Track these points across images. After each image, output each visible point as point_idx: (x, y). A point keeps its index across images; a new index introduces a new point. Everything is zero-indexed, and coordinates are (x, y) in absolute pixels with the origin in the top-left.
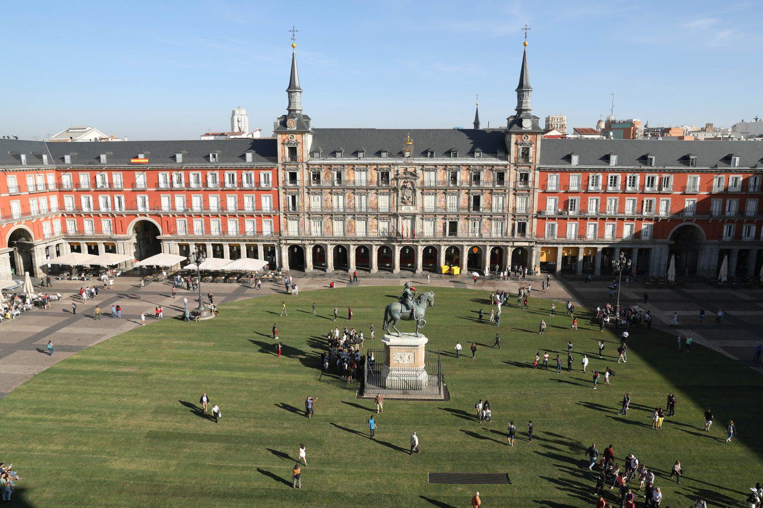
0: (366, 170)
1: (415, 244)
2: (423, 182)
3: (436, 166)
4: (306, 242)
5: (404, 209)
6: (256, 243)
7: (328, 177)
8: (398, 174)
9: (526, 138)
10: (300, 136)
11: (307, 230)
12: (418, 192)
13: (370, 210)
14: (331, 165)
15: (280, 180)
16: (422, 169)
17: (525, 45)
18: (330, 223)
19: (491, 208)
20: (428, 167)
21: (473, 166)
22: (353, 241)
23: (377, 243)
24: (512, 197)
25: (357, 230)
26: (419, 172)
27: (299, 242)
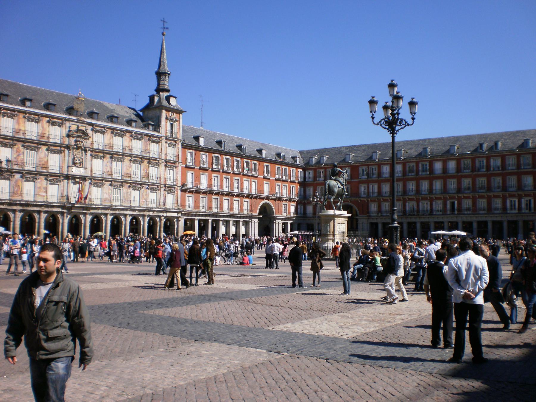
0: (37, 121)
2: (92, 144)
3: (104, 127)
5: (75, 171)
8: (70, 131)
12: (89, 153)
13: (40, 170)
16: (92, 130)
17: (163, 34)
21: (136, 133)
23: (46, 209)
24: (163, 167)
25: (25, 192)
26: (89, 132)
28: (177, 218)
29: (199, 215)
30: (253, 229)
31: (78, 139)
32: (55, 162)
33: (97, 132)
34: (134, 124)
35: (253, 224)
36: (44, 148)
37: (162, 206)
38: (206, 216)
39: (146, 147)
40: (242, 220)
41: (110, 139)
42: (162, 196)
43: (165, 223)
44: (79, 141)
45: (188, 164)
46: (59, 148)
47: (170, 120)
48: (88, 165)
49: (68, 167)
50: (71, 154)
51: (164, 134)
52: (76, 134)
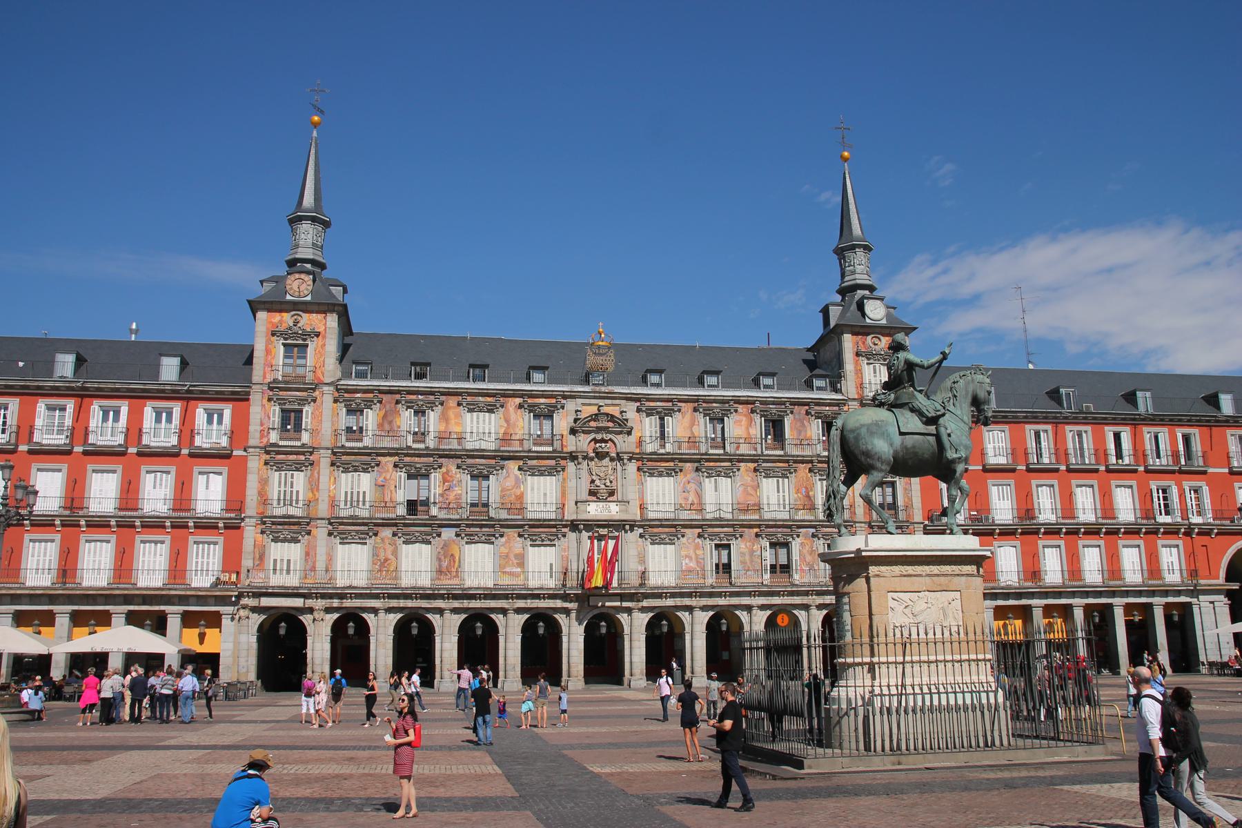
1: (625, 604)
2: (640, 442)
4: (319, 604)
5: (595, 510)
6: (162, 608)
7: (390, 423)
8: (576, 420)
9: (877, 341)
10: (320, 316)
11: (321, 565)
13: (504, 515)
14: (399, 392)
15: (254, 428)
18: (390, 549)
19: (812, 508)
20: (652, 404)
21: (762, 403)
22: (456, 597)
23: (521, 604)
27: (298, 602)
31: (599, 437)
32: (541, 495)
36: (513, 466)
38: (1019, 596)
39: (800, 432)
41: (692, 424)
44: (603, 441)
46: (553, 462)
48: (632, 494)
49: (576, 503)
50: (584, 473)
52: (593, 424)
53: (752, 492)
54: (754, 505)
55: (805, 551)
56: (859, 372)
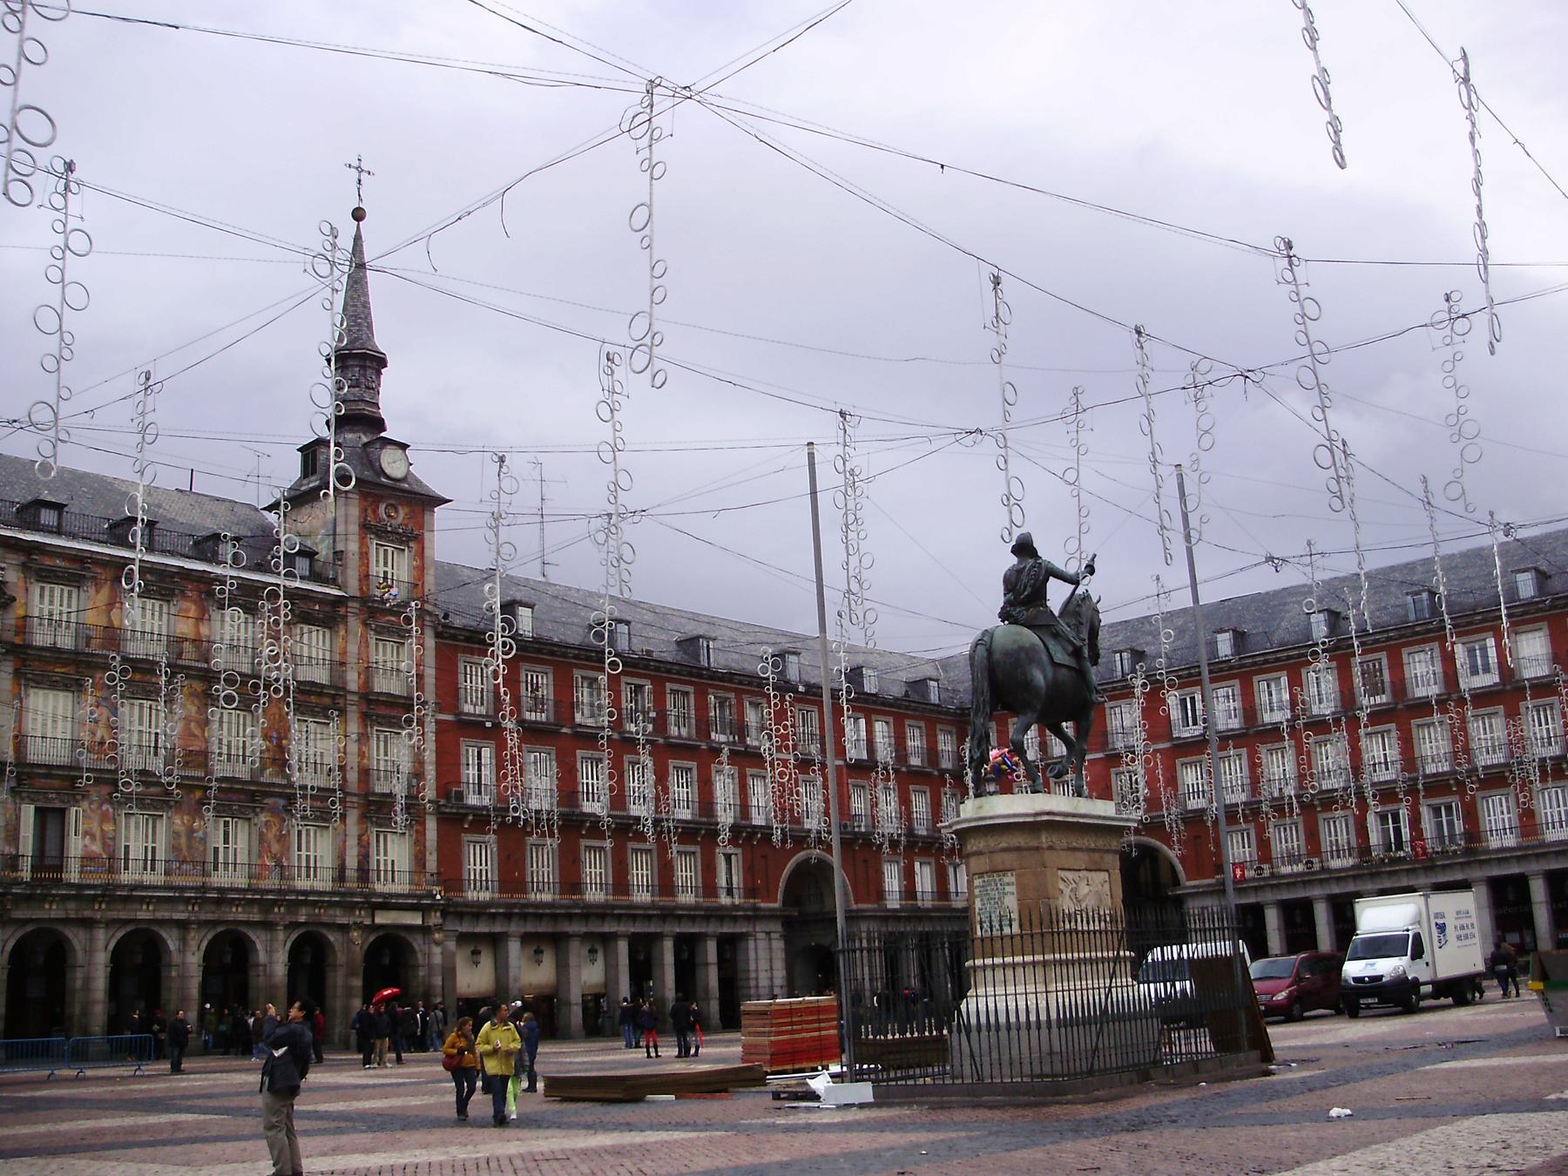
2: (23, 625)
19: (284, 763)
20: (48, 562)
24: (354, 728)
28: (424, 930)
29: (524, 917)
30: (763, 965)
33: (48, 576)
34: (227, 551)
35: (762, 944)
37: (351, 885)
38: (555, 917)
40: (713, 928)
41: (111, 605)
42: (352, 842)
43: (372, 954)
45: (468, 708)
47: (381, 533)
51: (353, 588)
53: (197, 732)
54: (198, 753)
55: (270, 836)
56: (364, 555)
